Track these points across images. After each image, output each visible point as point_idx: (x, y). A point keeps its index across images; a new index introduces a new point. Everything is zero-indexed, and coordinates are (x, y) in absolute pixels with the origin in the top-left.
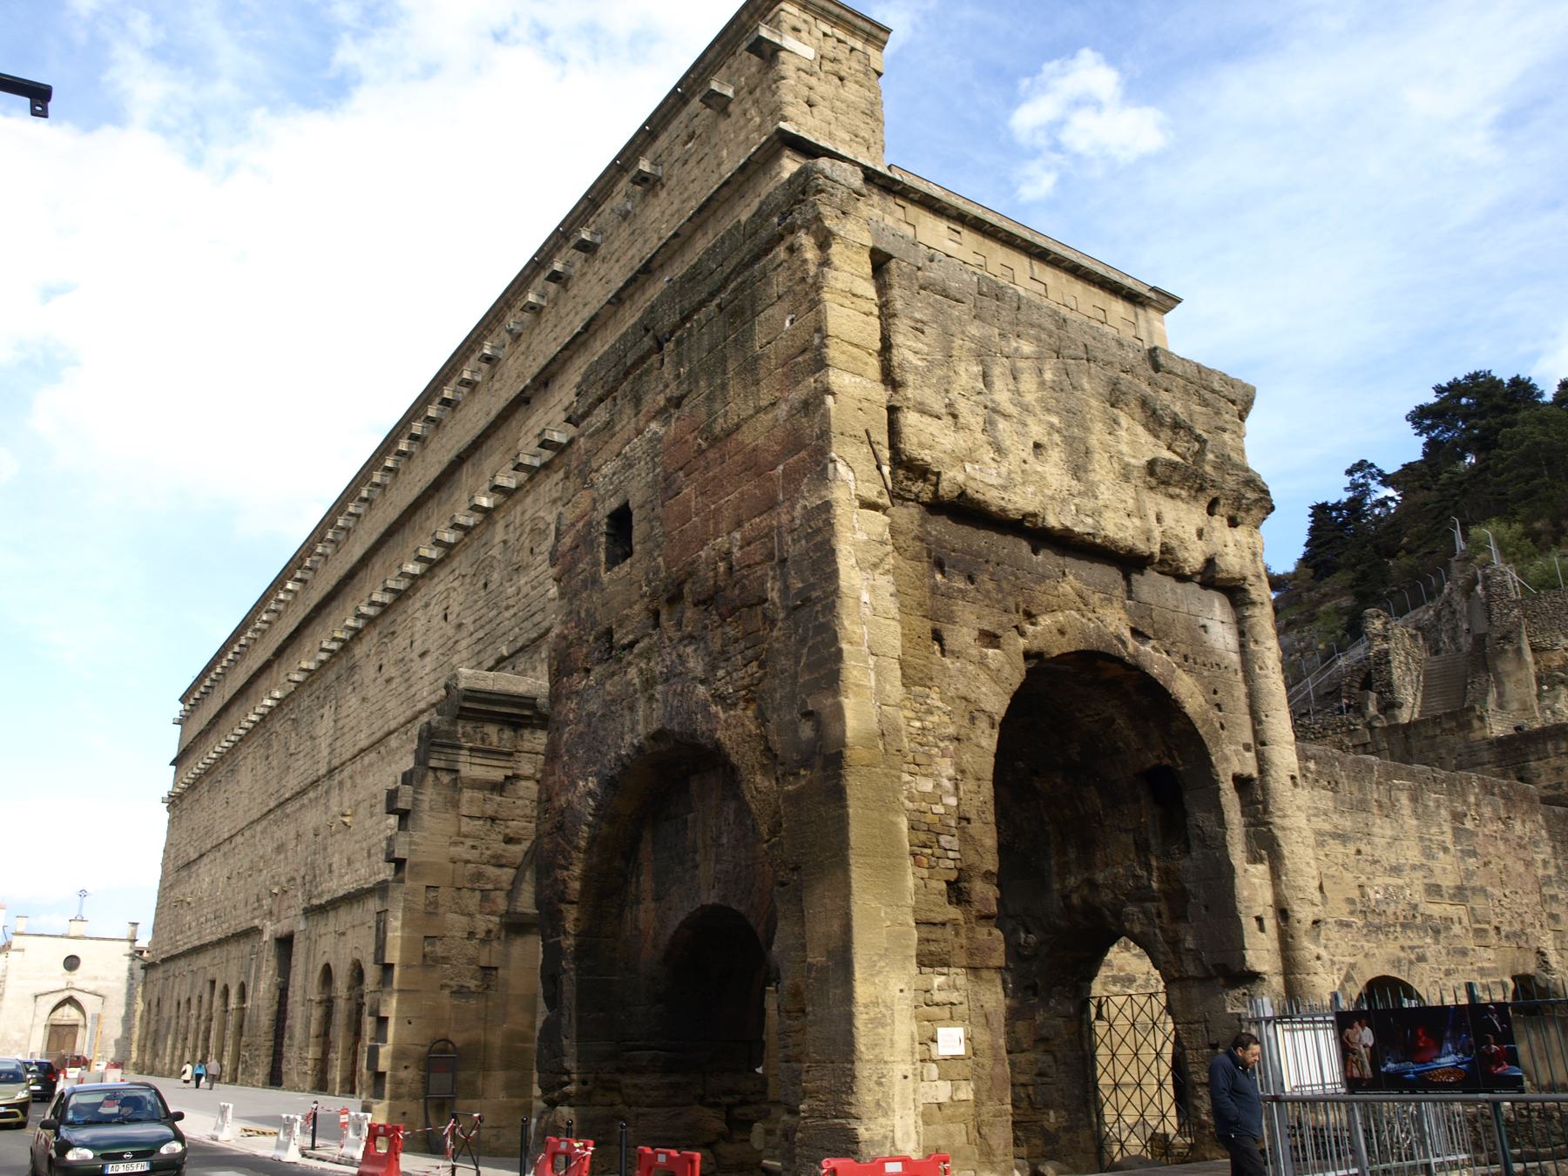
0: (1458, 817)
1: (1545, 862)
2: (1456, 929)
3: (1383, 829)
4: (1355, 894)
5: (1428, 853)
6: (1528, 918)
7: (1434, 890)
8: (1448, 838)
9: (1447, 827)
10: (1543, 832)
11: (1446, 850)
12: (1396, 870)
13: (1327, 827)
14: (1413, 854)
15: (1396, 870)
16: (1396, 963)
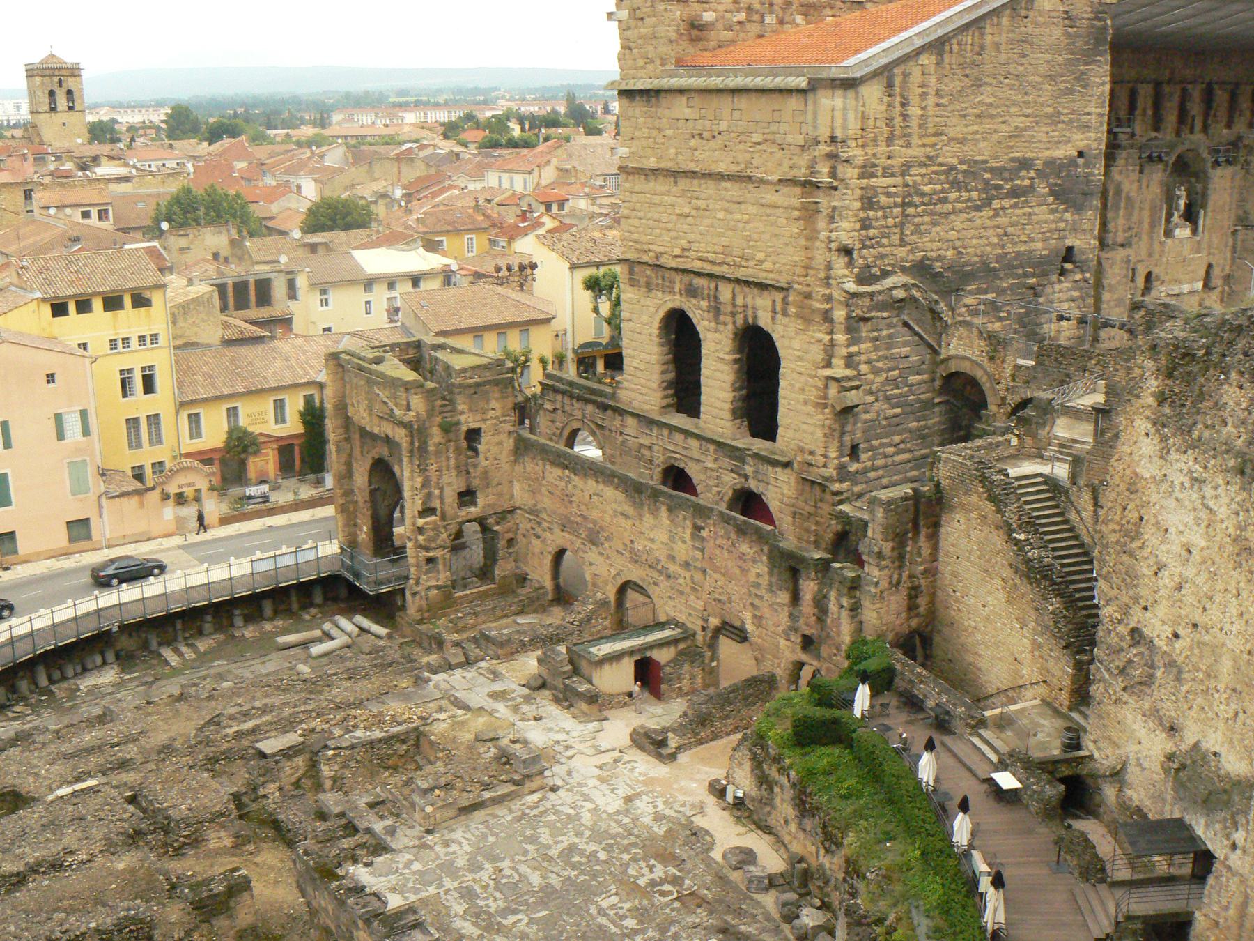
0: (697, 528)
1: (758, 575)
2: (681, 581)
3: (648, 519)
4: (628, 543)
5: (672, 539)
6: (733, 598)
7: (672, 558)
8: (687, 536)
9: (689, 531)
10: (765, 558)
11: (684, 542)
12: (652, 540)
13: (620, 509)
14: (663, 537)
15: (652, 540)
16: (643, 580)
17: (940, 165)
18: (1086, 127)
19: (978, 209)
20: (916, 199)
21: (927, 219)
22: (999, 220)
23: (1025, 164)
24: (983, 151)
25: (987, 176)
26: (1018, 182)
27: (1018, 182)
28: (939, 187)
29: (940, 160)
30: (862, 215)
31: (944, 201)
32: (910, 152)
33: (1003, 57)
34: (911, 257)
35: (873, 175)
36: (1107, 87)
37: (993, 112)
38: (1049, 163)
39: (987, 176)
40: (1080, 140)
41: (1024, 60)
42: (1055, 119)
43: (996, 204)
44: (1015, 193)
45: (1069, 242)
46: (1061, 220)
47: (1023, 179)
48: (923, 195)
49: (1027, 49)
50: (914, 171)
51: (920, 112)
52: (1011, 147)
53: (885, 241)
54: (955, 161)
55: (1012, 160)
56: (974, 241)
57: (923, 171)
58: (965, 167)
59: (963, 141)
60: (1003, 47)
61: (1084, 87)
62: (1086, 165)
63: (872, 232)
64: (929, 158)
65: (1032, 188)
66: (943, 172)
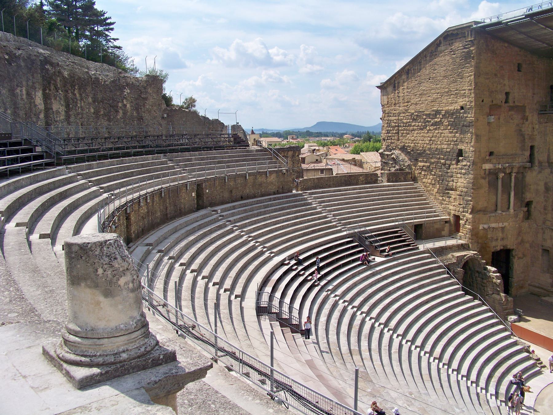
17: (409, 113)
18: (464, 96)
19: (422, 129)
21: (405, 132)
23: (438, 112)
24: (422, 107)
27: (436, 120)
31: (410, 126)
32: (401, 109)
34: (401, 145)
35: (390, 116)
36: (473, 77)
37: (425, 92)
38: (447, 112)
39: (424, 117)
40: (461, 102)
41: (435, 72)
42: (449, 93)
45: (459, 147)
46: (455, 137)
47: (438, 118)
48: (404, 123)
49: (437, 67)
52: (433, 106)
54: (413, 111)
55: (433, 111)
56: (420, 142)
57: (404, 115)
59: (416, 104)
61: (461, 79)
62: (465, 113)
66: (410, 115)
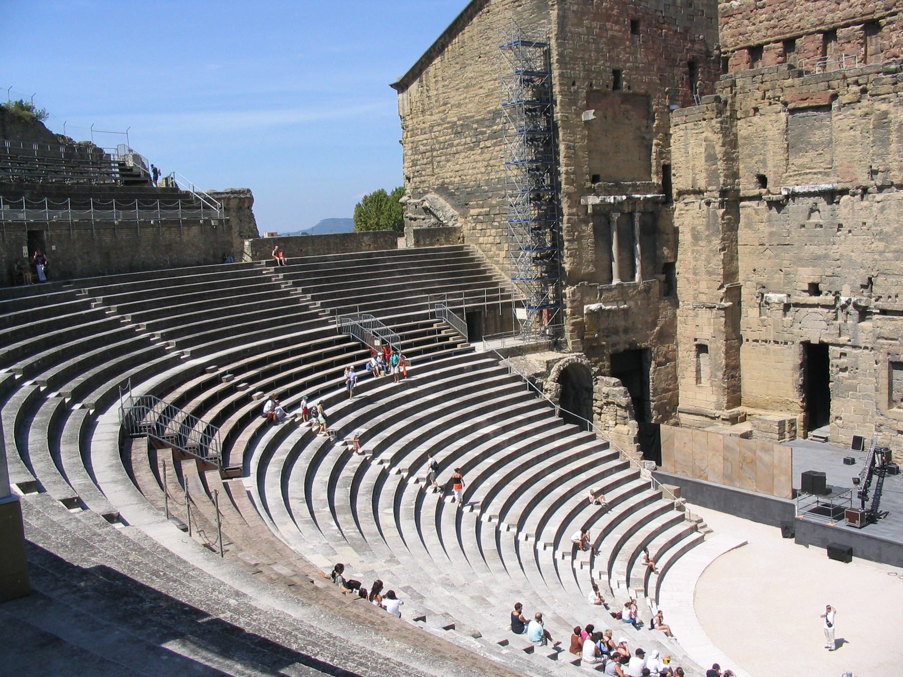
17: (448, 123)
19: (472, 149)
20: (437, 146)
22: (487, 156)
24: (470, 109)
25: (475, 126)
26: (495, 127)
27: (495, 127)
28: (448, 137)
29: (448, 120)
30: (412, 158)
31: (452, 145)
32: (433, 118)
33: (476, 45)
37: (474, 82)
39: (475, 126)
41: (489, 42)
43: (482, 145)
44: (494, 135)
47: (498, 125)
50: (435, 129)
51: (435, 92)
52: (488, 103)
53: (423, 173)
54: (455, 119)
55: (489, 112)
56: (470, 171)
57: (440, 128)
58: (461, 122)
59: (459, 105)
60: (475, 38)
63: (418, 168)
64: (442, 120)
65: (504, 130)
